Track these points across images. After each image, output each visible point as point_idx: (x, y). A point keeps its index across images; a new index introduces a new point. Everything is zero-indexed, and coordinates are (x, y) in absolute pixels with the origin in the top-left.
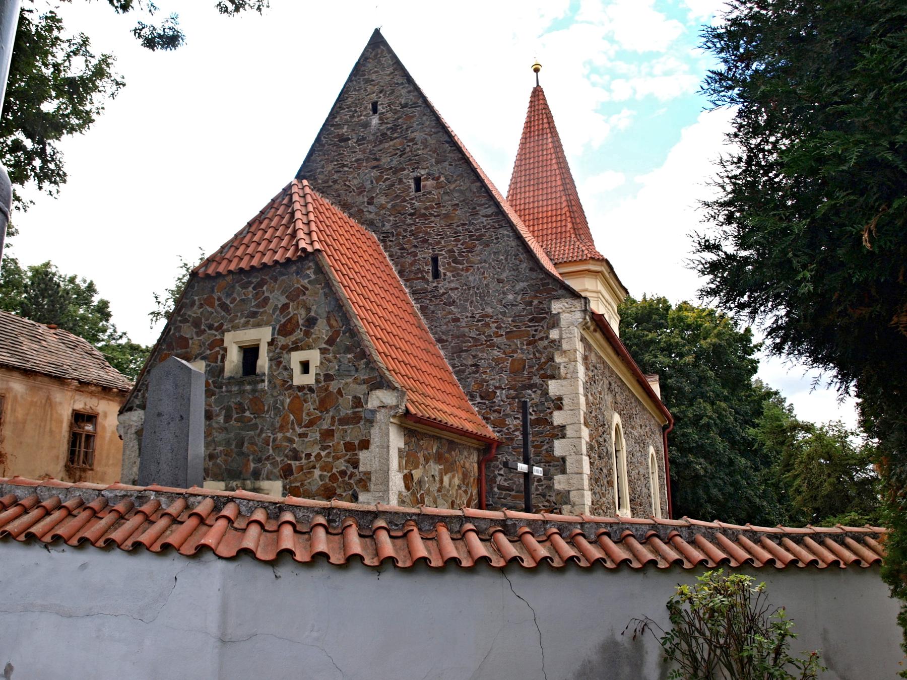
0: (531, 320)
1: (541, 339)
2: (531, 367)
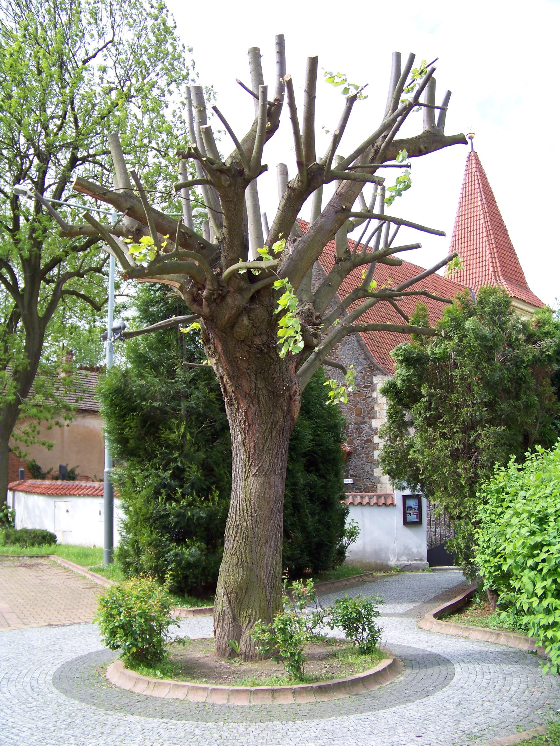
0: (364, 387)
1: (369, 397)
2: (364, 412)
